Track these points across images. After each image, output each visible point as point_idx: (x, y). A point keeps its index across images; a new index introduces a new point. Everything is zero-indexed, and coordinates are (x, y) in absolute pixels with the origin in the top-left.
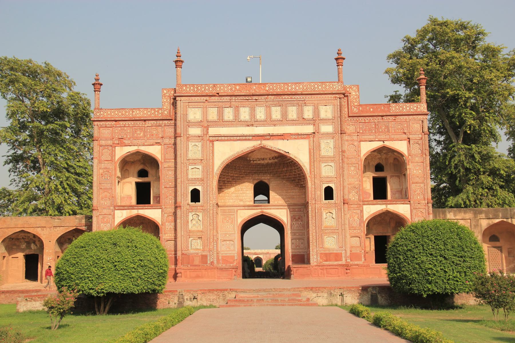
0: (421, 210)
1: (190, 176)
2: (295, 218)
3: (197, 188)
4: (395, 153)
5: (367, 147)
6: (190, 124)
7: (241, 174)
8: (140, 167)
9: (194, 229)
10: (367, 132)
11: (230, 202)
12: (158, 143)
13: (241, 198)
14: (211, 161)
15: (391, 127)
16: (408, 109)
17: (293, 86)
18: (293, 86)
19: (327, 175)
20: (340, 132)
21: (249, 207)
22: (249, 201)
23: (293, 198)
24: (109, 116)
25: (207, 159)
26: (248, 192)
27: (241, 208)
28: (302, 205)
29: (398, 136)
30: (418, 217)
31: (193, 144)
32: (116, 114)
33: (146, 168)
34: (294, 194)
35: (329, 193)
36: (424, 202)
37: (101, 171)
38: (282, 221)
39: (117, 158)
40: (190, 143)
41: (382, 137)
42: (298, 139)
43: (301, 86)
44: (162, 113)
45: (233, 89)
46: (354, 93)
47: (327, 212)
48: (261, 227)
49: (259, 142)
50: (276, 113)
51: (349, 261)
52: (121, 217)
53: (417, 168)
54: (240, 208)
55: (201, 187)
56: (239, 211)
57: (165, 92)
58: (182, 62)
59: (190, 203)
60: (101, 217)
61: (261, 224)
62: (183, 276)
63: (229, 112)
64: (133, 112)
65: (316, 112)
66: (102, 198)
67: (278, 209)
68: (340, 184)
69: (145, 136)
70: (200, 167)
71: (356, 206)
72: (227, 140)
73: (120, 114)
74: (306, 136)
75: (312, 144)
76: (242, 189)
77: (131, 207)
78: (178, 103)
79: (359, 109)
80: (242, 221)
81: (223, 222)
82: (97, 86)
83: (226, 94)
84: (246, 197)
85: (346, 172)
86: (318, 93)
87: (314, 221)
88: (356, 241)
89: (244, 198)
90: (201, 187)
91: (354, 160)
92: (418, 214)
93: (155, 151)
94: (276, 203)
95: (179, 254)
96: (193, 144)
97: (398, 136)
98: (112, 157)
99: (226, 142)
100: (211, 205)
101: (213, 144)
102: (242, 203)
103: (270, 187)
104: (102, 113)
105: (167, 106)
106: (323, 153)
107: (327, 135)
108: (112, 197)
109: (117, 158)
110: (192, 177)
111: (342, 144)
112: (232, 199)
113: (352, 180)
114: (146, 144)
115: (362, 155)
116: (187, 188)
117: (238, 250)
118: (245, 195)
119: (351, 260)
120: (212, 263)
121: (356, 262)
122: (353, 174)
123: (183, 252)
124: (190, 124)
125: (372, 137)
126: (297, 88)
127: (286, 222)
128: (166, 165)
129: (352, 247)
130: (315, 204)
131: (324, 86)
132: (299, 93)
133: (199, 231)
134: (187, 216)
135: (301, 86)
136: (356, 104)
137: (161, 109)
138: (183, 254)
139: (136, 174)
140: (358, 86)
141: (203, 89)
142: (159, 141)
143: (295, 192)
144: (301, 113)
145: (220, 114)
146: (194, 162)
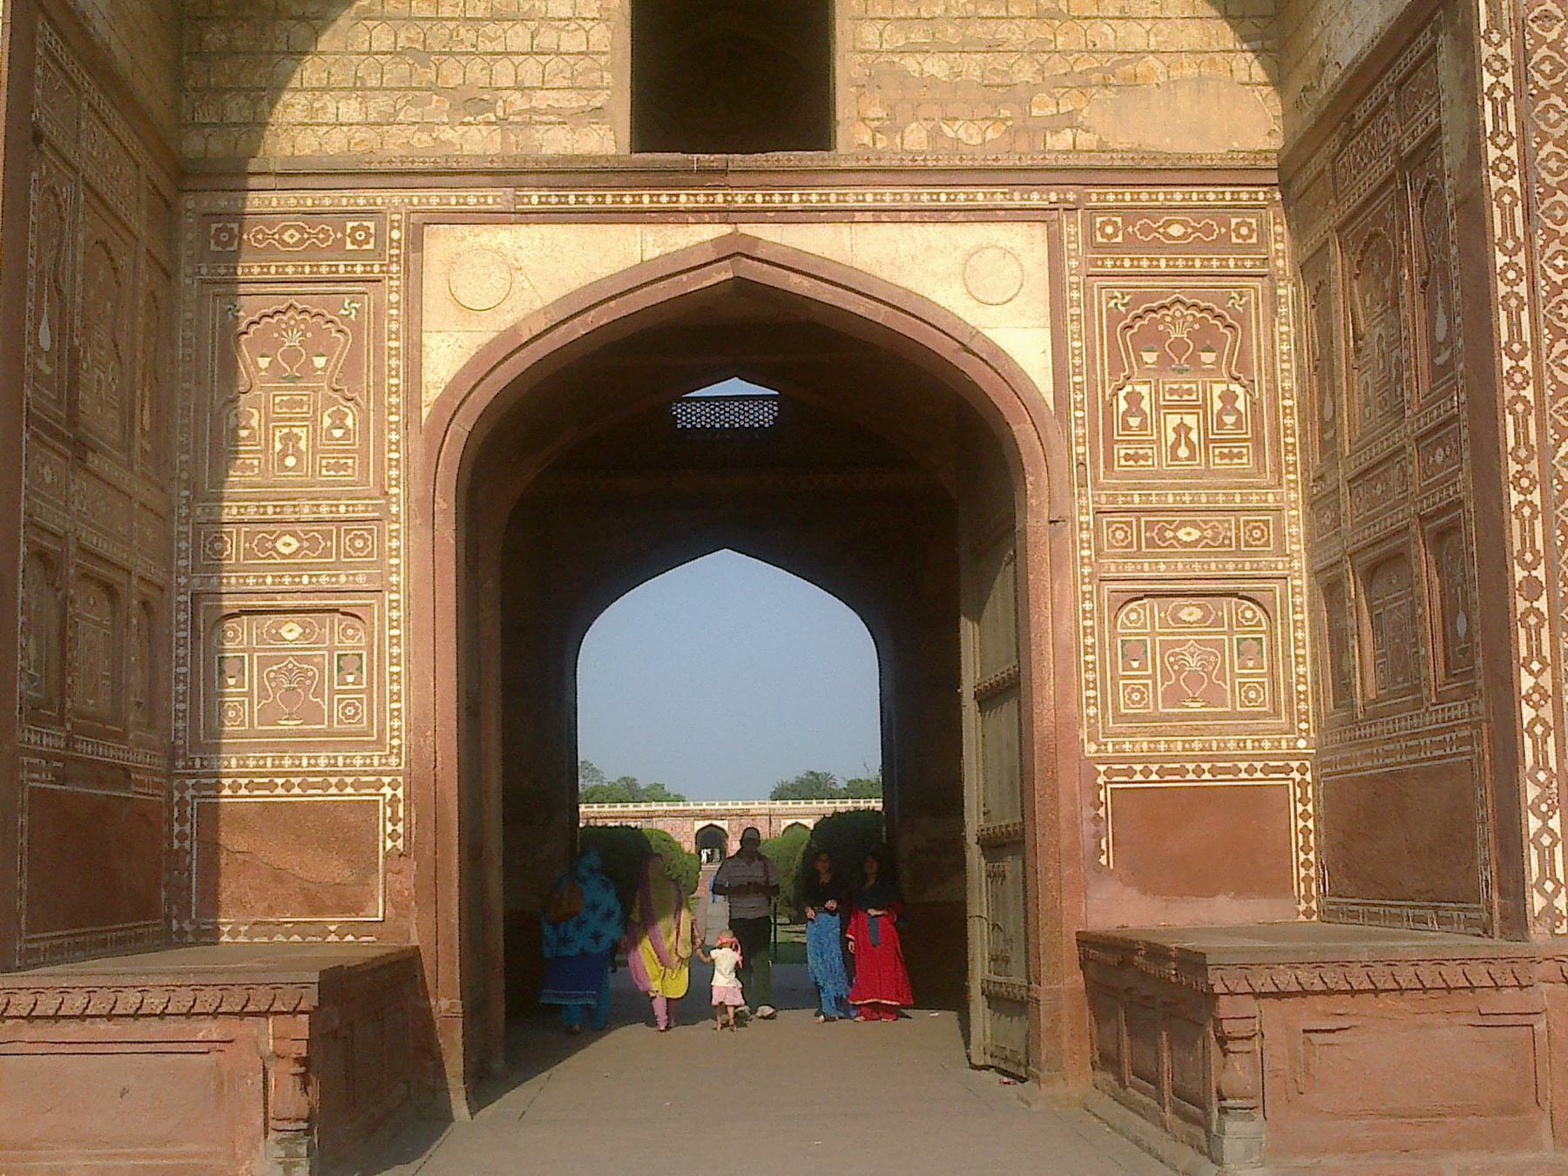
2: (1151, 339)
13: (477, 72)
23: (1132, 83)
27: (472, 199)
38: (996, 360)
54: (452, 199)
56: (441, 244)
61: (726, 553)
84: (531, 70)
94: (915, 138)
102: (476, 141)
112: (358, 88)
118: (518, 37)
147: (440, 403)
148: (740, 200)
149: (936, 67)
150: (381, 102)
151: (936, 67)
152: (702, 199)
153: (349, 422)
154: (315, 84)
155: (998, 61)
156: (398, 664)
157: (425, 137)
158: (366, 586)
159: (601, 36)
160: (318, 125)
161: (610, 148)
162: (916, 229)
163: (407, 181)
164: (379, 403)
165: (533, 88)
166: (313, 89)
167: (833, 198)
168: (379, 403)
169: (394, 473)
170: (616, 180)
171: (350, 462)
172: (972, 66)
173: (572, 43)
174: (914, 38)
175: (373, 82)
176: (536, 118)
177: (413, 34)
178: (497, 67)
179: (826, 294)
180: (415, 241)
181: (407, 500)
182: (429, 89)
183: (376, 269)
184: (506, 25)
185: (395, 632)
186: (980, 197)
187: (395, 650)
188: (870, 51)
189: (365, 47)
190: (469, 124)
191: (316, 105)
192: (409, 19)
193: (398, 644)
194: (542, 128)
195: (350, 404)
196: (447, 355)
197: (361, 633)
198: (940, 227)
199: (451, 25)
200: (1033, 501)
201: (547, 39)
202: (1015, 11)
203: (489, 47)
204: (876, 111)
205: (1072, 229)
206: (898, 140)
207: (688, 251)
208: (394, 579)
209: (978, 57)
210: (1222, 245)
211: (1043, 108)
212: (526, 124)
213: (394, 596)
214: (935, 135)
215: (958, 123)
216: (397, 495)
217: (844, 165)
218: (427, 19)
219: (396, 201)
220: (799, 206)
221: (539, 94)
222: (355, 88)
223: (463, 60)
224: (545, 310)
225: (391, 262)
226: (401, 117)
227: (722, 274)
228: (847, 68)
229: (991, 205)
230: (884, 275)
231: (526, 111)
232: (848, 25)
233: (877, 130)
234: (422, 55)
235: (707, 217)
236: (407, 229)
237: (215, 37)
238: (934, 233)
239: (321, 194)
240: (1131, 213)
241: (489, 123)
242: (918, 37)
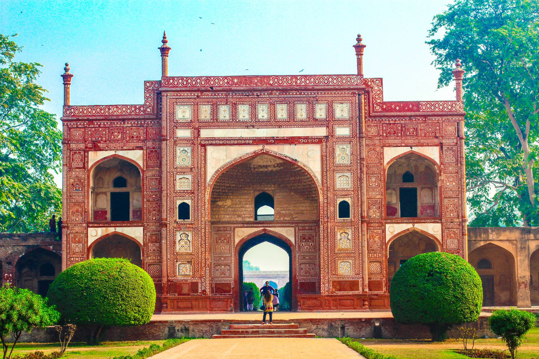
0: (455, 230)
1: (178, 188)
2: (304, 238)
3: (187, 201)
4: (426, 161)
5: (391, 154)
6: (178, 125)
8: (117, 174)
9: (183, 250)
10: (392, 135)
11: (226, 218)
12: (141, 148)
14: (203, 169)
15: (421, 130)
16: (441, 107)
17: (303, 80)
18: (303, 80)
19: (342, 187)
20: (358, 136)
24: (81, 114)
25: (198, 167)
26: (248, 206)
28: (314, 223)
29: (429, 141)
30: (450, 238)
31: (182, 149)
32: (90, 112)
33: (124, 176)
34: (303, 209)
35: (344, 209)
36: (457, 220)
37: (72, 181)
39: (90, 165)
40: (178, 148)
41: (411, 141)
42: (308, 143)
43: (312, 80)
44: (144, 111)
45: (230, 83)
46: (376, 88)
47: (341, 231)
48: (266, 247)
49: (261, 147)
50: (282, 112)
51: (367, 290)
52: (96, 236)
53: (451, 180)
55: (190, 201)
56: (237, 230)
57: (148, 85)
58: (169, 49)
59: (178, 220)
60: (72, 236)
62: (169, 307)
63: (225, 111)
64: (109, 109)
65: (330, 111)
66: (73, 213)
67: (284, 227)
68: (358, 198)
69: (123, 138)
70: (189, 177)
71: (377, 225)
72: (223, 145)
73: (94, 112)
74: (319, 141)
75: (324, 150)
76: (240, 202)
77: (107, 225)
78: (164, 99)
79: (382, 107)
80: (241, 241)
81: (217, 242)
82: (67, 78)
83: (221, 88)
85: (365, 185)
86: (332, 87)
87: (325, 243)
88: (375, 267)
89: (242, 213)
90: (190, 201)
91: (375, 169)
92: (450, 234)
93: (136, 156)
94: (282, 219)
95: (165, 280)
96: (182, 149)
97: (429, 141)
98: (84, 164)
99: (222, 147)
100: (203, 223)
101: (205, 149)
102: (240, 219)
103: (275, 200)
104: (72, 110)
105: (151, 102)
106: (338, 160)
107: (343, 139)
108: (85, 212)
109: (90, 165)
110: (180, 189)
111: (360, 151)
112: (228, 214)
113: (372, 194)
114: (125, 148)
115: (385, 163)
116: (174, 202)
117: (235, 276)
118: (244, 209)
119: (370, 290)
120: (204, 291)
121: (376, 292)
122: (374, 186)
123: (170, 278)
124: (178, 125)
125: (397, 141)
126: (308, 82)
127: (294, 242)
128: (149, 174)
129: (370, 274)
130: (327, 222)
131: (340, 79)
132: (310, 87)
133: (187, 254)
134: (174, 236)
135: (312, 80)
136: (379, 101)
137: (142, 106)
138: (169, 281)
139: (111, 184)
140: (381, 80)
141: (194, 83)
142: (140, 144)
143: (305, 206)
144: (311, 111)
145: (215, 112)
146: (183, 171)
147: (237, 245)
149: (284, 212)
150: (230, 216)
151: (284, 212)
159: (251, 209)
172: (287, 212)
173: (249, 210)
179: (273, 235)
196: (237, 241)
205: (297, 228)
210: (311, 229)
211: (294, 216)
234: (234, 211)
237: (214, 209)
240: (303, 227)
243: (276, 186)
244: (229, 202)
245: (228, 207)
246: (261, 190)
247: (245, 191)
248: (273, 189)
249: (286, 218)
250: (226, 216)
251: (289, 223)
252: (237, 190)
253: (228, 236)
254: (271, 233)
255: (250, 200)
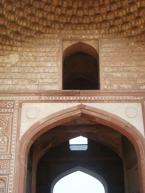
7: (35, 24)
13: (33, 76)
21: (50, 96)
22: (49, 84)
26: (49, 64)
27: (32, 98)
54: (28, 98)
56: (25, 106)
61: (79, 172)
67: (120, 101)
76: (35, 57)
84: (43, 75)
94: (115, 87)
102: (33, 87)
112: (12, 78)
118: (41, 70)
147: (23, 136)
148: (82, 98)
149: (119, 75)
151: (119, 75)
152: (75, 98)
153: (5, 140)
154: (3, 78)
155: (130, 74)
156: (11, 190)
157: (23, 87)
158: (6, 173)
159: (56, 70)
160: (4, 85)
161: (58, 89)
162: (116, 104)
163: (19, 95)
164: (11, 136)
165: (44, 79)
166: (3, 79)
167: (100, 98)
168: (11, 136)
169: (13, 150)
170: (59, 95)
171: (5, 148)
172: (126, 75)
174: (114, 70)
175: (14, 77)
176: (45, 84)
177: (22, 69)
178: (37, 75)
179: (99, 116)
180: (20, 106)
181: (15, 156)
182: (24, 79)
183: (13, 111)
184: (39, 68)
185: (11, 183)
186: (128, 98)
187: (11, 187)
188: (106, 72)
189: (13, 71)
190: (32, 85)
191: (4, 81)
192: (22, 67)
193: (11, 186)
194: (45, 86)
195: (6, 136)
197: (4, 184)
198: (121, 103)
199: (29, 68)
200: (142, 157)
201: (47, 70)
202: (133, 65)
203: (36, 71)
204: (107, 82)
206: (112, 87)
207: (72, 108)
208: (11, 172)
209: (126, 73)
211: (139, 82)
212: (42, 85)
213: (11, 176)
214: (119, 87)
215: (123, 85)
216: (13, 155)
217: (102, 92)
218: (24, 67)
219: (17, 98)
220: (93, 99)
221: (45, 79)
222: (11, 78)
223: (31, 74)
224: (44, 119)
225: (15, 109)
226: (19, 84)
227: (79, 112)
228: (102, 75)
229: (130, 99)
230: (110, 112)
231: (42, 83)
232: (102, 68)
233: (108, 86)
234: (24, 73)
235: (76, 102)
236: (19, 103)
238: (119, 104)
239: (3, 97)
241: (35, 85)
242: (115, 69)
243: (103, 31)
244: (14, 58)
245: (13, 66)
246: (75, 39)
247: (45, 41)
248: (96, 37)
249: (125, 86)
250: (6, 82)
251: (129, 93)
252: (31, 37)
253: (7, 118)
254: (93, 114)
255: (54, 54)
